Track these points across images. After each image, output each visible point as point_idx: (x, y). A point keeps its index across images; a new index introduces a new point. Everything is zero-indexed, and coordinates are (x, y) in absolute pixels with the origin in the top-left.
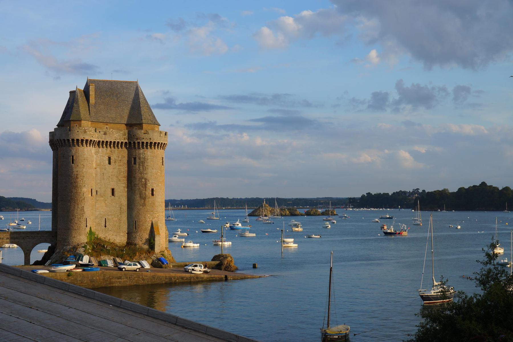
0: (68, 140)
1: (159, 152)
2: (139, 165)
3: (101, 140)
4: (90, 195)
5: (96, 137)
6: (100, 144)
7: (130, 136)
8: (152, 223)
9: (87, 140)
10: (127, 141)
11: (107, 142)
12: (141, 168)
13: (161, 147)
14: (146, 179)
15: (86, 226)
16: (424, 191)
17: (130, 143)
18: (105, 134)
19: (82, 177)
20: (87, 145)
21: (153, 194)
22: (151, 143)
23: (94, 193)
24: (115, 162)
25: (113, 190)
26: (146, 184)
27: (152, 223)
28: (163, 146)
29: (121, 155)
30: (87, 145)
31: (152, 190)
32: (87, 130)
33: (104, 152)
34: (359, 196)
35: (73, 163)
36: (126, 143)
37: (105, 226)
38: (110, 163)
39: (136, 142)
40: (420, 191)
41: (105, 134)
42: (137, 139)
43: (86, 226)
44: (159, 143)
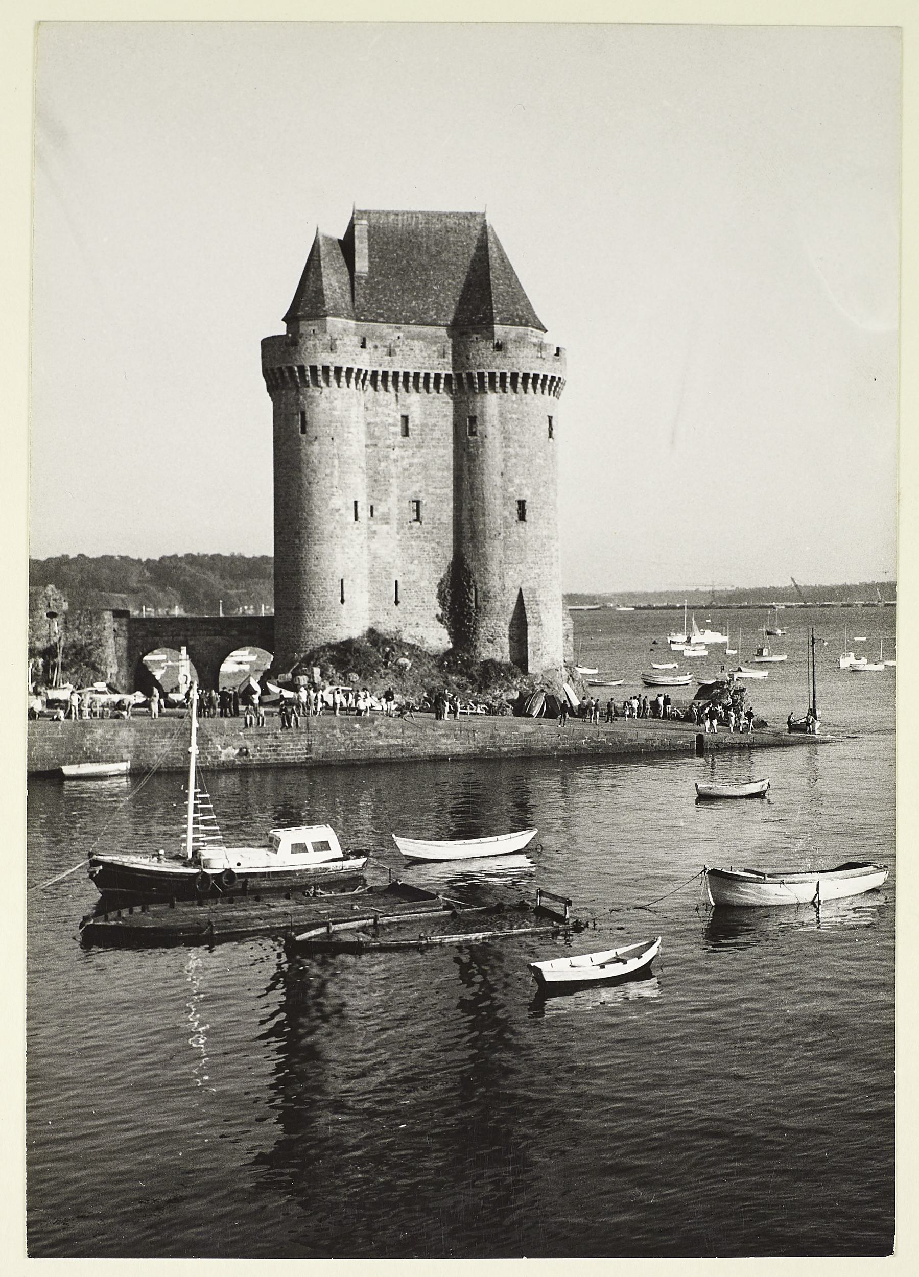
0: (291, 369)
1: (537, 402)
5: (364, 361)
7: (460, 357)
8: (520, 596)
9: (338, 370)
13: (543, 385)
15: (342, 601)
17: (459, 376)
19: (328, 471)
20: (338, 381)
23: (364, 513)
27: (520, 596)
28: (552, 385)
29: (434, 411)
30: (338, 381)
32: (342, 341)
35: (304, 431)
36: (448, 376)
37: (397, 602)
39: (475, 373)
42: (479, 367)
43: (342, 601)
44: (536, 377)
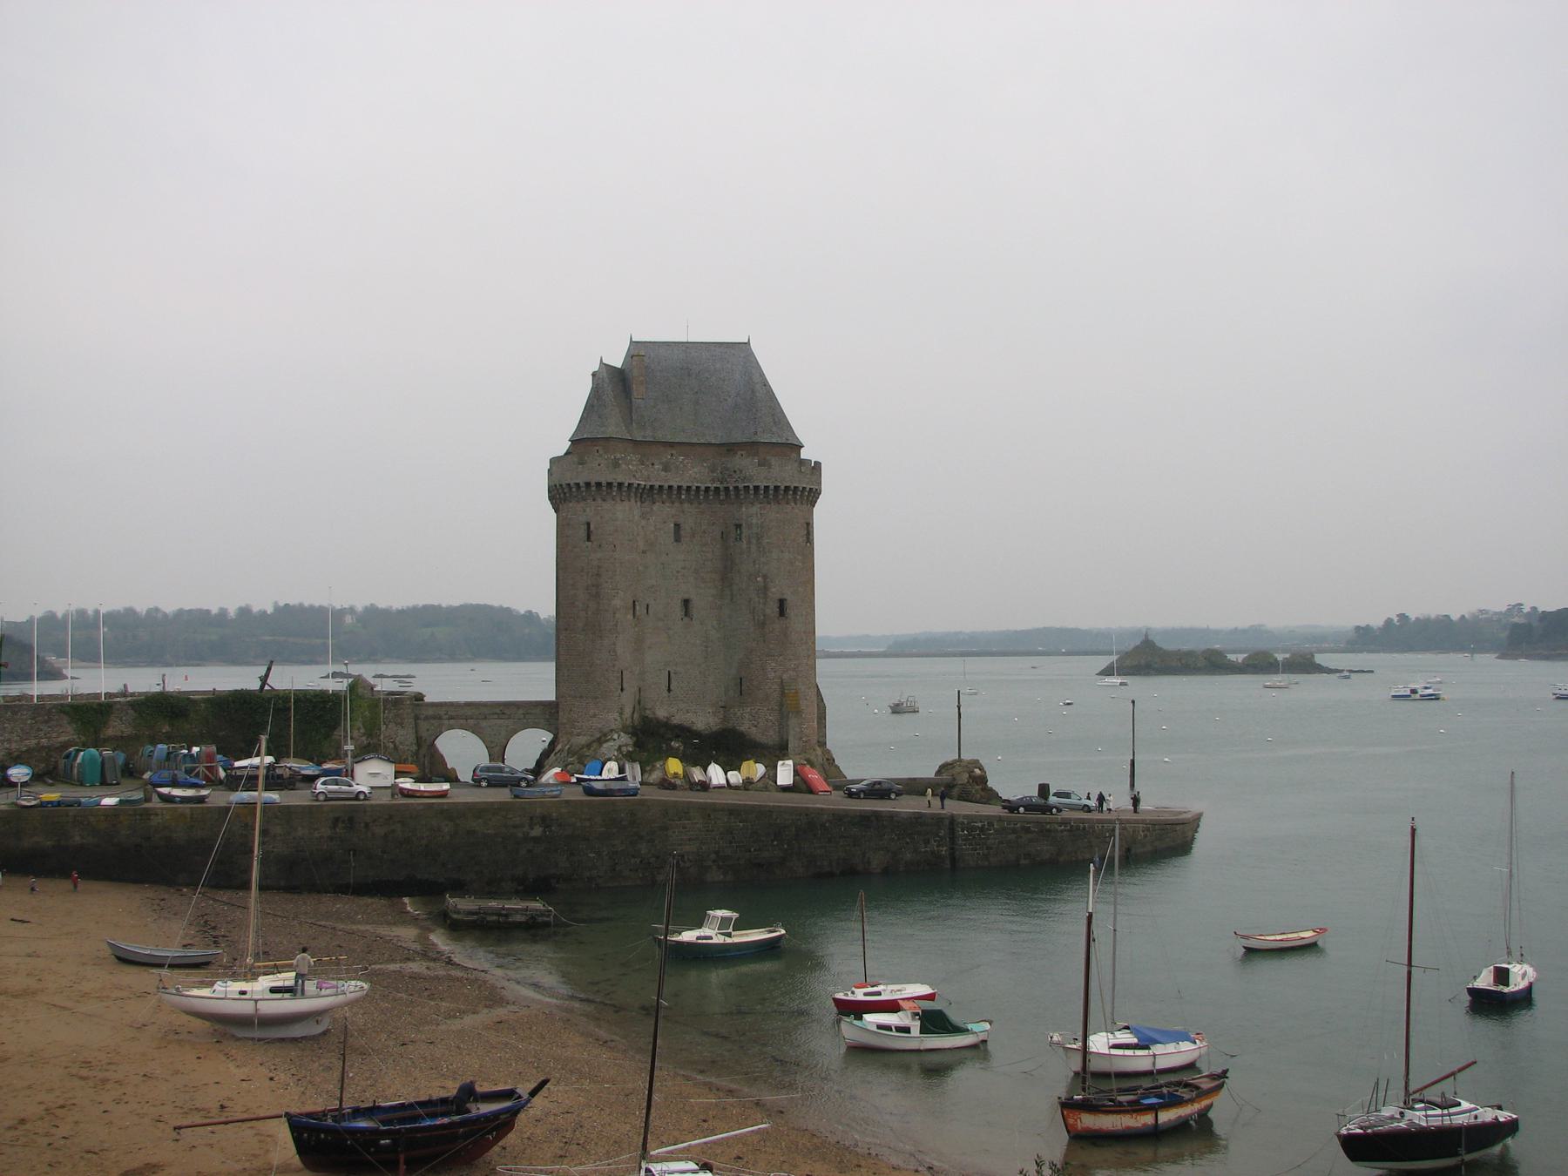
2: (749, 542)
3: (657, 484)
4: (630, 617)
6: (648, 493)
10: (717, 484)
11: (670, 487)
12: (754, 548)
14: (765, 577)
16: (1534, 609)
18: (666, 469)
21: (782, 612)
22: (777, 488)
24: (693, 536)
25: (686, 602)
26: (766, 589)
31: (782, 602)
33: (664, 513)
34: (1377, 622)
38: (678, 539)
39: (741, 486)
40: (1526, 609)
41: (666, 469)
